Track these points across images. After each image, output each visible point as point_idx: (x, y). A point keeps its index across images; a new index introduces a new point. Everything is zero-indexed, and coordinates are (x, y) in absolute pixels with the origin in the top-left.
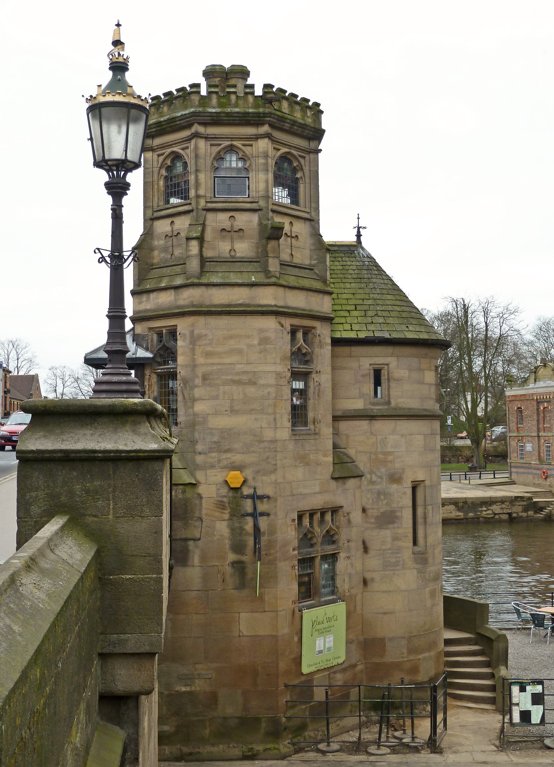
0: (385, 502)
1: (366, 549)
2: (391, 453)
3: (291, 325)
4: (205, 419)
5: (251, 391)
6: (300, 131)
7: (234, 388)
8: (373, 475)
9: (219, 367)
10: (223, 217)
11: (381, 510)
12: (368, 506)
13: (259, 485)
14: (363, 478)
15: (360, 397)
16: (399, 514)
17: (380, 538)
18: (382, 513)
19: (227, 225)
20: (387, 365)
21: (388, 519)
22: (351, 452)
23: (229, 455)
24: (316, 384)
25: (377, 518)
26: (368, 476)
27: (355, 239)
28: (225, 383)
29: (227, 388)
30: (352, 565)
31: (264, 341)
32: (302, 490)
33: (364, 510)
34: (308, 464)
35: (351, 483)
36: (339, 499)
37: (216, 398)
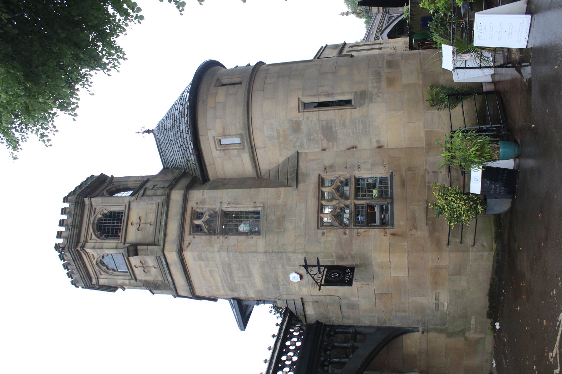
0: (315, 135)
1: (354, 147)
2: (278, 132)
3: (190, 234)
4: (259, 292)
5: (234, 266)
6: (78, 219)
7: (234, 275)
8: (296, 144)
9: (224, 283)
10: (137, 271)
11: (322, 137)
12: (321, 148)
13: (297, 263)
14: (300, 151)
15: (241, 156)
16: (324, 123)
17: (345, 138)
18: (325, 137)
19: (141, 269)
20: (214, 138)
21: (328, 132)
22: (281, 160)
23: (280, 280)
24: (229, 206)
25: (329, 141)
26: (297, 148)
27: (151, 134)
28: (233, 280)
29: (236, 279)
30: (365, 163)
31: (201, 258)
32: (302, 224)
33: (324, 150)
34: (284, 217)
35: (302, 165)
36: (313, 180)
37: (244, 286)
